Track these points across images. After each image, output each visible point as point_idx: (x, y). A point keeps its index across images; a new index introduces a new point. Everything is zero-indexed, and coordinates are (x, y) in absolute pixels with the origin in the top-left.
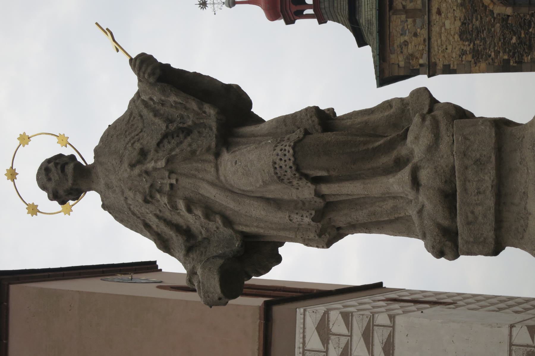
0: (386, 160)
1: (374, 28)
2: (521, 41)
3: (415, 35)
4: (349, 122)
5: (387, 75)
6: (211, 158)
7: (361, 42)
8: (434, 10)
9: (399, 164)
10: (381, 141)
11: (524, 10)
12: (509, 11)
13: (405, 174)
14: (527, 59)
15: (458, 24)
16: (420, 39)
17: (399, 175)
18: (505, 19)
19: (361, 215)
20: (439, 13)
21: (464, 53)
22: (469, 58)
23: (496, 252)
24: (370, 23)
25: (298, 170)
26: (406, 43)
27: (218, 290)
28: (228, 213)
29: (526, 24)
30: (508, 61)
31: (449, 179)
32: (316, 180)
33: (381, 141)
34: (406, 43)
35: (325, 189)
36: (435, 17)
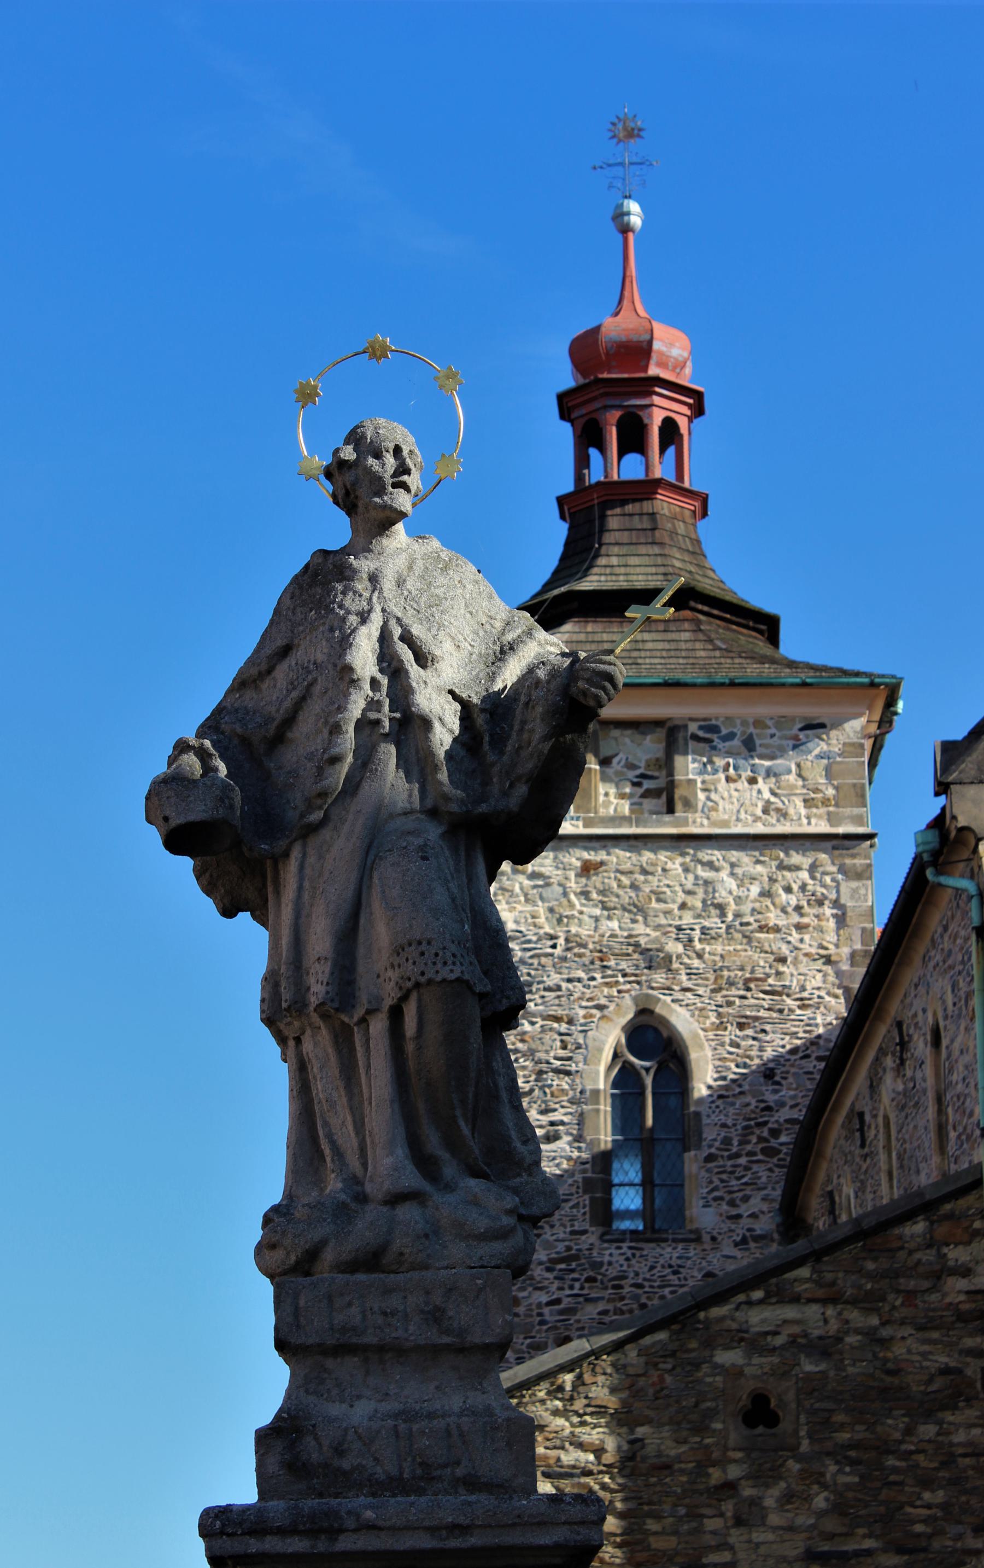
0: (433, 1141)
4: (497, 1065)
6: (429, 803)
9: (425, 1163)
10: (465, 1130)
13: (411, 1179)
17: (410, 1167)
19: (326, 1085)
23: (281, 1345)
25: (417, 985)
28: (326, 833)
33: (465, 1130)
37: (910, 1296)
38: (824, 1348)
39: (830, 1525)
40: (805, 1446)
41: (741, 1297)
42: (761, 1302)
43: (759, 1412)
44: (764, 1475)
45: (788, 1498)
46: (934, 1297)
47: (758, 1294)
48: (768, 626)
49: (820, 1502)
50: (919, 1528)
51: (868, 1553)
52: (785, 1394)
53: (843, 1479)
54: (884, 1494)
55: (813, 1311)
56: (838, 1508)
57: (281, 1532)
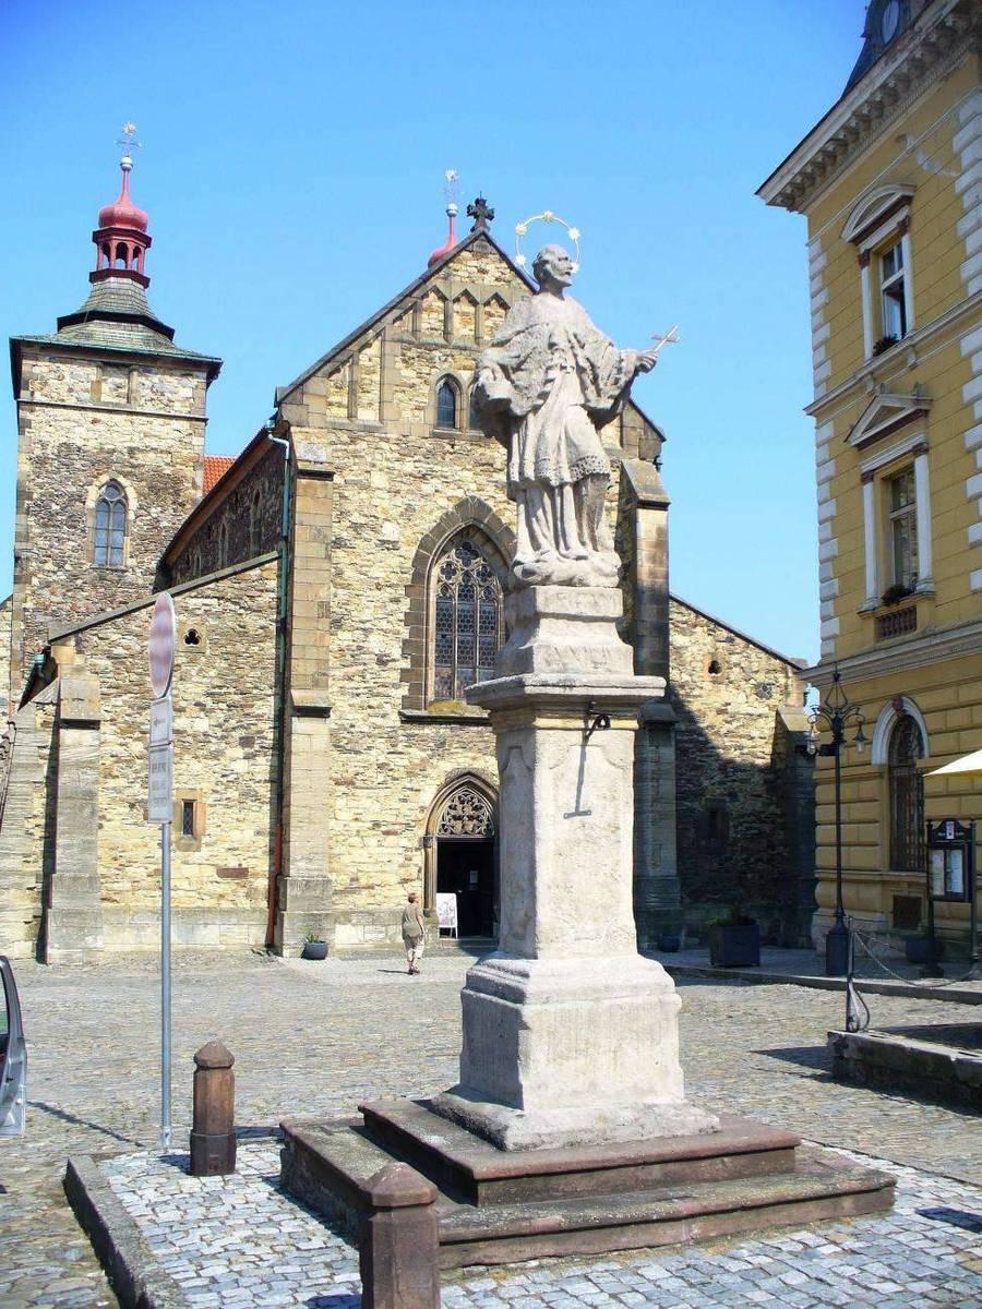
1: (83, 342)
2: (52, 515)
3: (71, 390)
5: (25, 350)
7: (64, 322)
8: (98, 415)
11: (90, 522)
12: (91, 504)
14: (31, 520)
15: (79, 443)
16: (65, 395)
18: (81, 499)
20: (94, 421)
21: (44, 446)
22: (38, 452)
24: (89, 336)
26: (60, 378)
27: (496, 397)
29: (73, 522)
30: (30, 498)
31: (582, 583)
32: (576, 486)
34: (60, 378)
35: (568, 491)
36: (91, 415)
37: (251, 597)
38: (218, 616)
39: (217, 682)
40: (208, 652)
41: (187, 594)
42: (195, 597)
43: (192, 638)
44: (192, 661)
45: (201, 670)
46: (260, 599)
47: (193, 594)
48: (168, 333)
49: (213, 673)
50: (249, 685)
51: (230, 693)
52: (202, 632)
53: (222, 665)
54: (238, 672)
55: (214, 602)
56: (220, 676)
57: (554, 686)
